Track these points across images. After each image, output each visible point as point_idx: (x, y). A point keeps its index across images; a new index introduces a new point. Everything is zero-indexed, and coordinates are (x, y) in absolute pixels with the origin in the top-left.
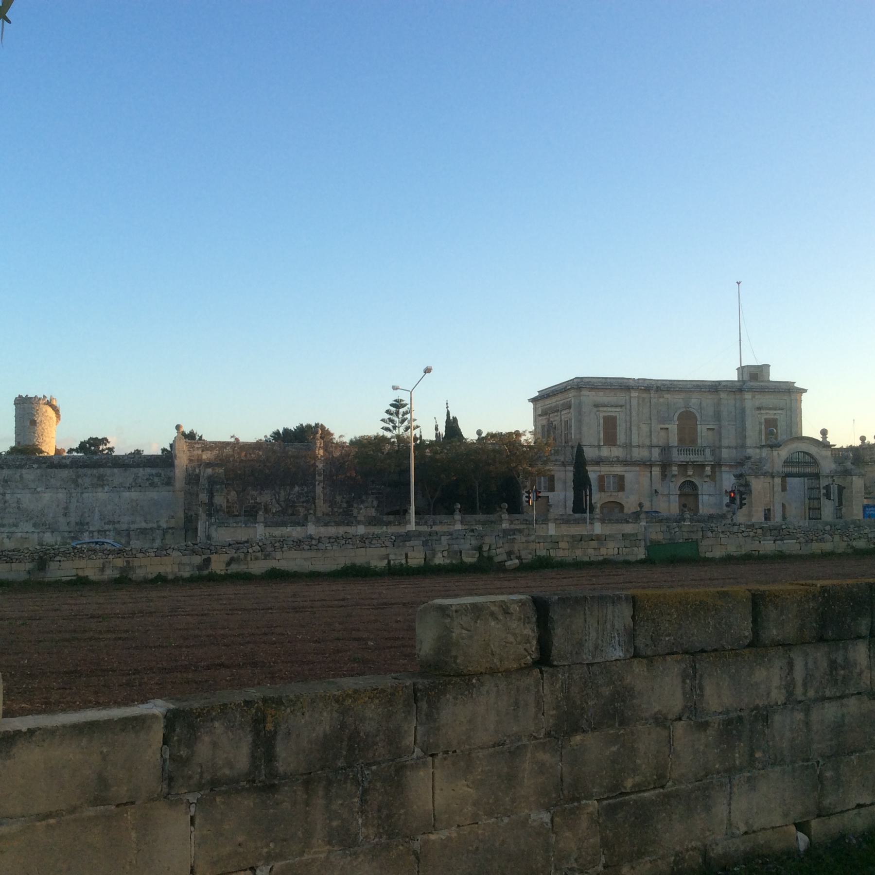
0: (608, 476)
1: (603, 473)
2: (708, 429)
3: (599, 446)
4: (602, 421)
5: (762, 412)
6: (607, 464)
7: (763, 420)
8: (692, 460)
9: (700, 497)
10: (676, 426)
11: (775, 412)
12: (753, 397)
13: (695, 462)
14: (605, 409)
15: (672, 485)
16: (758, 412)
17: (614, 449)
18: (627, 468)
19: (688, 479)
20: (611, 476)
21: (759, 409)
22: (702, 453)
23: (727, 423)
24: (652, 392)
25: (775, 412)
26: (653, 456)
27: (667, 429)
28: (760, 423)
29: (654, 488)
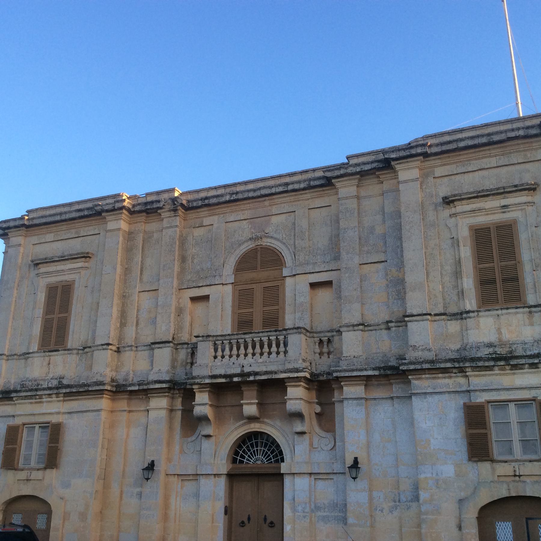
0: (31, 426)
1: (18, 421)
2: (313, 285)
3: (26, 355)
4: (42, 297)
5: (461, 207)
6: (26, 397)
7: (464, 233)
8: (247, 370)
9: (287, 480)
10: (230, 287)
11: (504, 202)
12: (425, 176)
13: (249, 374)
14: (52, 268)
15: (206, 445)
16: (446, 212)
17: (58, 358)
18: (75, 405)
19: (255, 427)
20: (37, 426)
21: (448, 201)
22: (282, 349)
23: (357, 260)
24: (165, 214)
25: (504, 202)
26: (156, 369)
27: (206, 298)
28: (455, 243)
29: (149, 459)
